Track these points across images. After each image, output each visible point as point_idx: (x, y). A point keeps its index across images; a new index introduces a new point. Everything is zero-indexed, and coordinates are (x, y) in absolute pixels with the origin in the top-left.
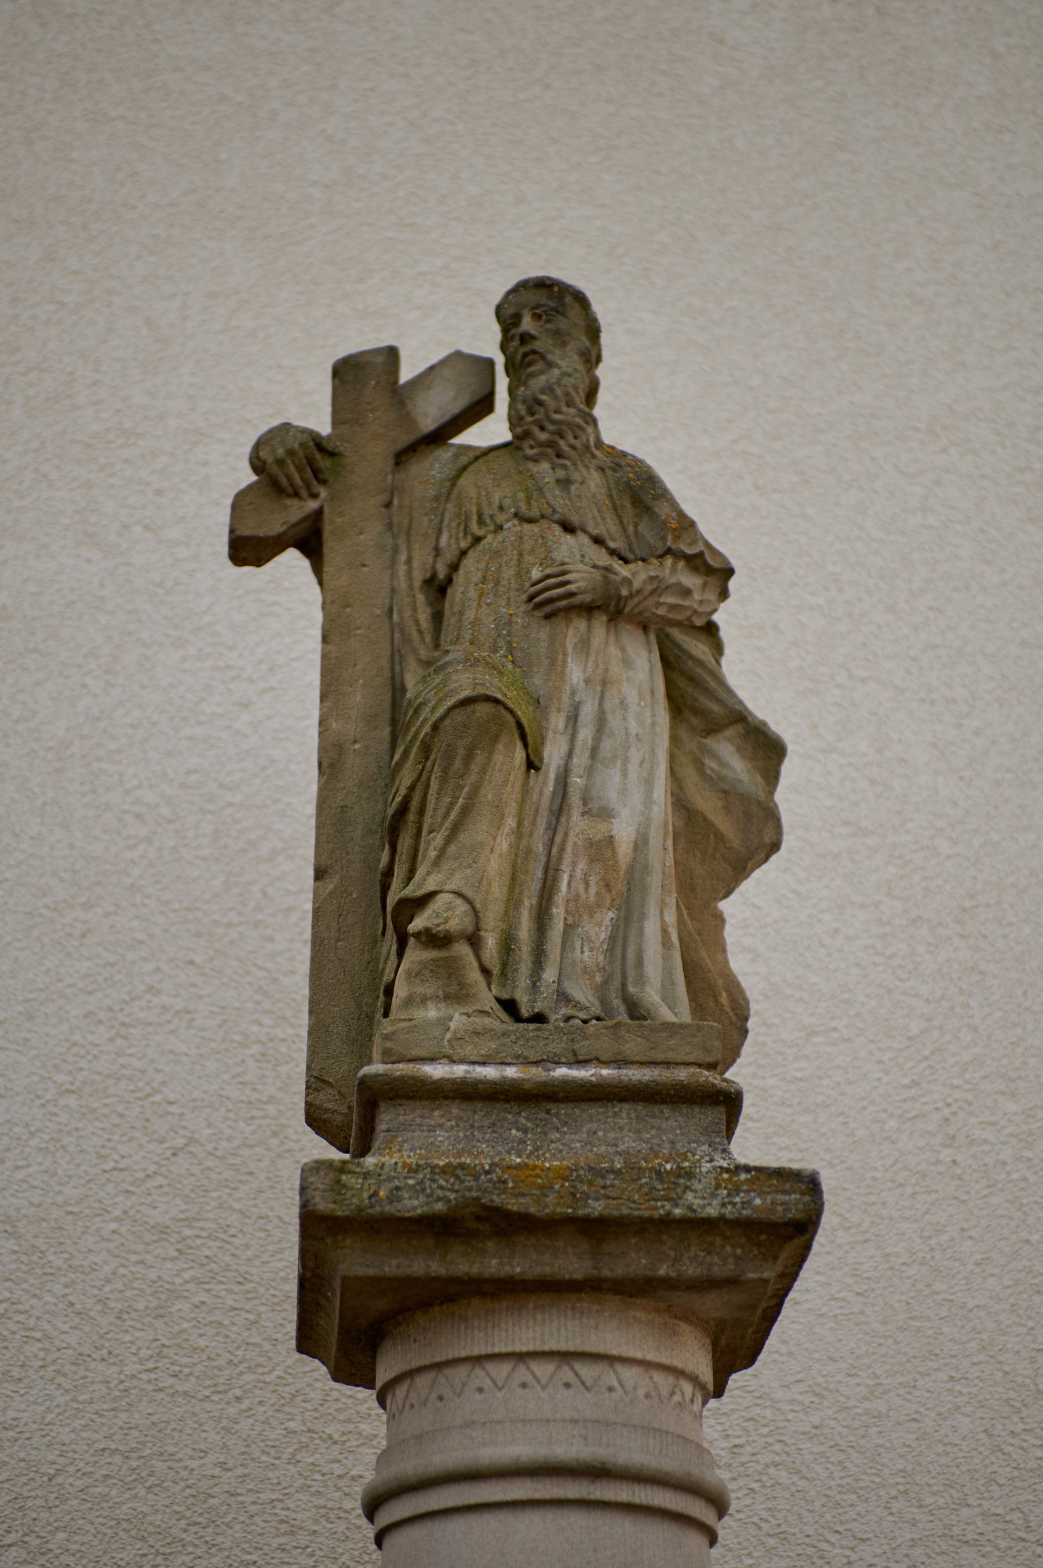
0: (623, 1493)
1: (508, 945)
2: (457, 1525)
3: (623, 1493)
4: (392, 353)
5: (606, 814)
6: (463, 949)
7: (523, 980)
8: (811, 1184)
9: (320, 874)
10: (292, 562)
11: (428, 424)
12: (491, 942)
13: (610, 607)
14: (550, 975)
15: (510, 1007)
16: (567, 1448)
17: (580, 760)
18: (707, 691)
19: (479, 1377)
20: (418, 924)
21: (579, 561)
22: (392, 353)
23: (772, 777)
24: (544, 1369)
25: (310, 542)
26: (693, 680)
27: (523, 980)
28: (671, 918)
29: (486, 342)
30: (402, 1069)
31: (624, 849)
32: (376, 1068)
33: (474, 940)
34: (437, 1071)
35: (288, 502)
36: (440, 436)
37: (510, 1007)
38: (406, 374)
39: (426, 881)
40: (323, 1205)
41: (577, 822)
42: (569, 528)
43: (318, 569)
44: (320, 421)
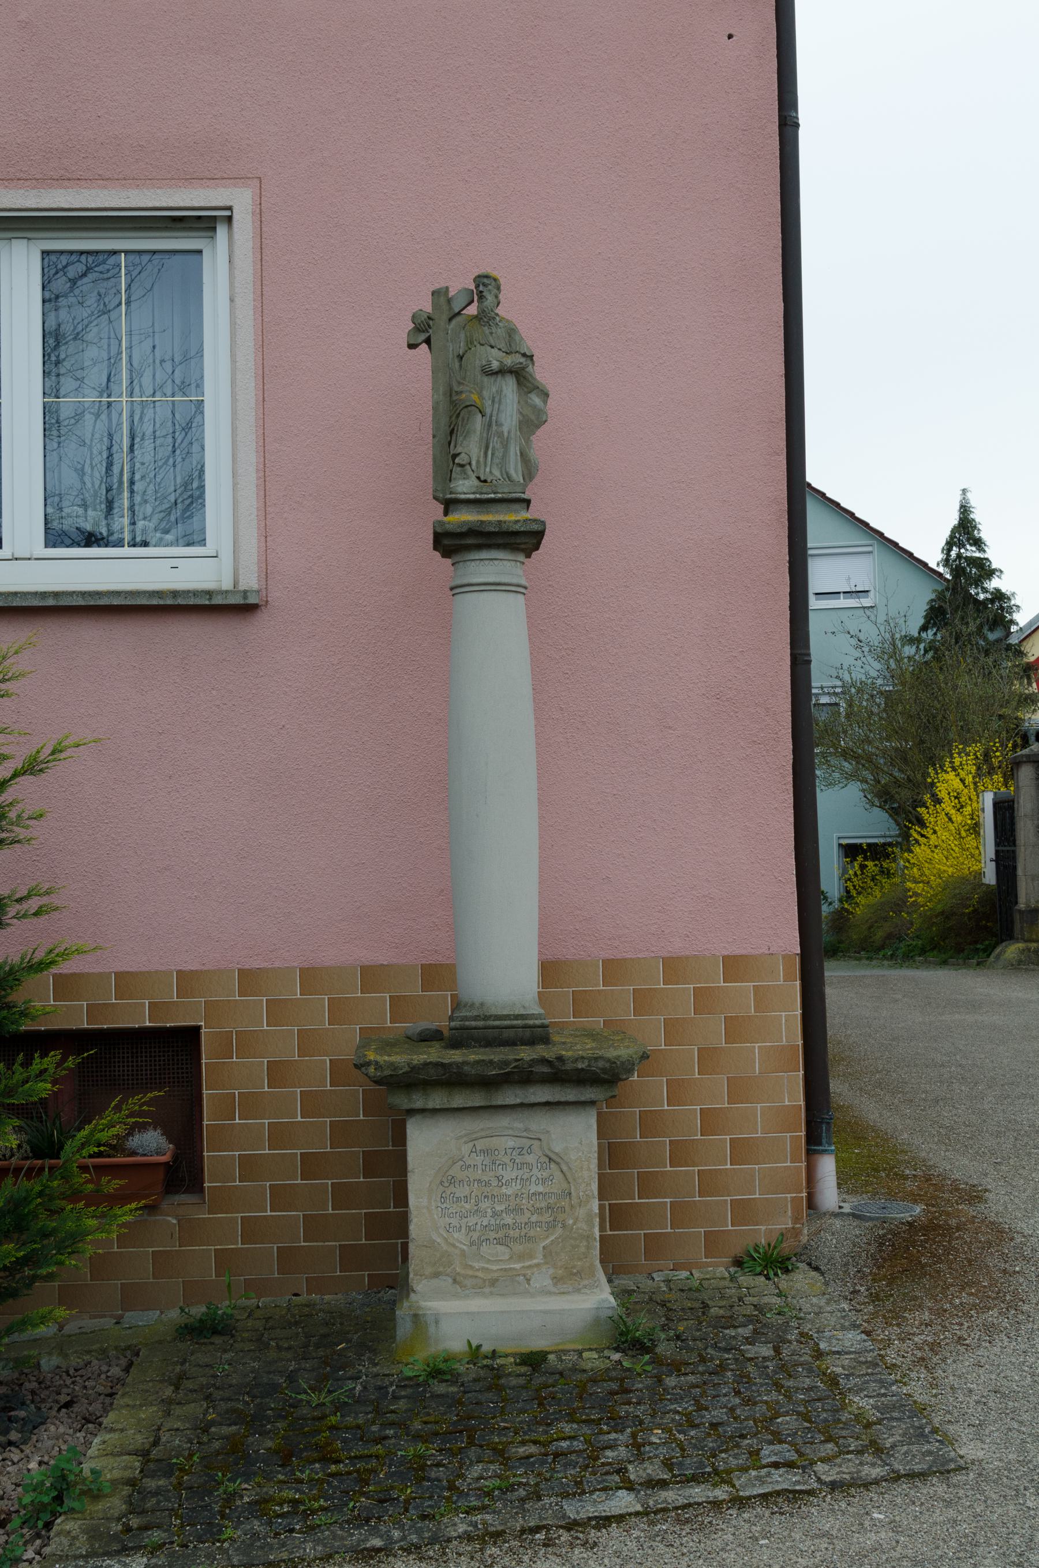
0: (504, 588)
1: (478, 462)
2: (469, 595)
3: (504, 588)
4: (447, 288)
5: (501, 425)
6: (468, 467)
7: (482, 471)
8: (543, 523)
9: (434, 437)
10: (424, 346)
11: (457, 310)
12: (474, 463)
13: (502, 372)
14: (488, 470)
15: (478, 478)
16: (491, 580)
17: (495, 413)
18: (529, 381)
19: (473, 563)
20: (457, 461)
21: (495, 358)
22: (447, 288)
23: (545, 402)
24: (487, 562)
25: (428, 341)
26: (524, 378)
27: (482, 471)
28: (518, 449)
29: (472, 287)
30: (453, 496)
31: (506, 434)
32: (449, 496)
33: (470, 464)
34: (463, 496)
35: (423, 332)
36: (459, 313)
37: (478, 478)
38: (451, 294)
39: (459, 449)
40: (439, 530)
41: (494, 428)
42: (492, 347)
43: (430, 348)
44: (428, 308)
